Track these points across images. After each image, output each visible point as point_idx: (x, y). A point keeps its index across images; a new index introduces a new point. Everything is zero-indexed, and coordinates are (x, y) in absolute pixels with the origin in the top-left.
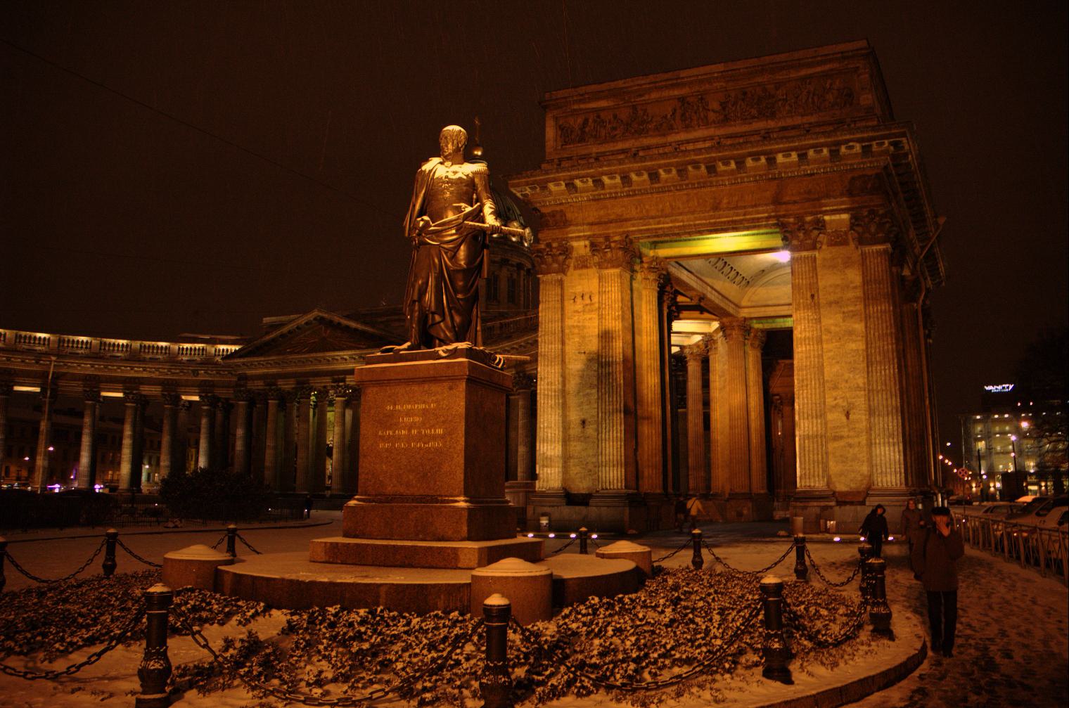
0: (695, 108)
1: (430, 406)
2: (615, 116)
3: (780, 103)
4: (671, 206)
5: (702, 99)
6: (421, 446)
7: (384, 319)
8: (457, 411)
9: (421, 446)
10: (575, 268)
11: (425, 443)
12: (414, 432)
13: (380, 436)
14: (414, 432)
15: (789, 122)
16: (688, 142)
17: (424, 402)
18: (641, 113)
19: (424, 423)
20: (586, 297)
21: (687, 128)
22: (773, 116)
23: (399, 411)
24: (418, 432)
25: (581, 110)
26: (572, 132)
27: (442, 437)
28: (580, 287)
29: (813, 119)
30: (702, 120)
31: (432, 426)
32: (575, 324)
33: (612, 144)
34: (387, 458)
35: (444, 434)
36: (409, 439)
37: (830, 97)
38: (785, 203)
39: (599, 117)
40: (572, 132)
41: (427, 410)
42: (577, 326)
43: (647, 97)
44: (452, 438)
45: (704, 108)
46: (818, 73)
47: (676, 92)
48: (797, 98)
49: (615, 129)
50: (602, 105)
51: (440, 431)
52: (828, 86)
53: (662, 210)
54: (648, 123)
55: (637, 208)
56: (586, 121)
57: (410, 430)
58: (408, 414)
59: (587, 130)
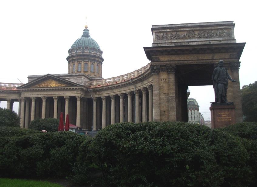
2: (171, 34)
7: (68, 77)
10: (161, 72)
12: (225, 118)
14: (225, 118)
15: (215, 39)
18: (178, 33)
19: (227, 116)
20: (165, 79)
21: (190, 38)
22: (211, 37)
25: (162, 31)
27: (231, 119)
29: (221, 39)
32: (162, 86)
36: (224, 119)
38: (215, 59)
39: (167, 33)
42: (162, 87)
43: (180, 30)
45: (194, 34)
46: (222, 28)
47: (187, 29)
49: (171, 37)
51: (230, 117)
52: (224, 31)
53: (184, 59)
56: (163, 34)
58: (223, 114)
59: (164, 36)
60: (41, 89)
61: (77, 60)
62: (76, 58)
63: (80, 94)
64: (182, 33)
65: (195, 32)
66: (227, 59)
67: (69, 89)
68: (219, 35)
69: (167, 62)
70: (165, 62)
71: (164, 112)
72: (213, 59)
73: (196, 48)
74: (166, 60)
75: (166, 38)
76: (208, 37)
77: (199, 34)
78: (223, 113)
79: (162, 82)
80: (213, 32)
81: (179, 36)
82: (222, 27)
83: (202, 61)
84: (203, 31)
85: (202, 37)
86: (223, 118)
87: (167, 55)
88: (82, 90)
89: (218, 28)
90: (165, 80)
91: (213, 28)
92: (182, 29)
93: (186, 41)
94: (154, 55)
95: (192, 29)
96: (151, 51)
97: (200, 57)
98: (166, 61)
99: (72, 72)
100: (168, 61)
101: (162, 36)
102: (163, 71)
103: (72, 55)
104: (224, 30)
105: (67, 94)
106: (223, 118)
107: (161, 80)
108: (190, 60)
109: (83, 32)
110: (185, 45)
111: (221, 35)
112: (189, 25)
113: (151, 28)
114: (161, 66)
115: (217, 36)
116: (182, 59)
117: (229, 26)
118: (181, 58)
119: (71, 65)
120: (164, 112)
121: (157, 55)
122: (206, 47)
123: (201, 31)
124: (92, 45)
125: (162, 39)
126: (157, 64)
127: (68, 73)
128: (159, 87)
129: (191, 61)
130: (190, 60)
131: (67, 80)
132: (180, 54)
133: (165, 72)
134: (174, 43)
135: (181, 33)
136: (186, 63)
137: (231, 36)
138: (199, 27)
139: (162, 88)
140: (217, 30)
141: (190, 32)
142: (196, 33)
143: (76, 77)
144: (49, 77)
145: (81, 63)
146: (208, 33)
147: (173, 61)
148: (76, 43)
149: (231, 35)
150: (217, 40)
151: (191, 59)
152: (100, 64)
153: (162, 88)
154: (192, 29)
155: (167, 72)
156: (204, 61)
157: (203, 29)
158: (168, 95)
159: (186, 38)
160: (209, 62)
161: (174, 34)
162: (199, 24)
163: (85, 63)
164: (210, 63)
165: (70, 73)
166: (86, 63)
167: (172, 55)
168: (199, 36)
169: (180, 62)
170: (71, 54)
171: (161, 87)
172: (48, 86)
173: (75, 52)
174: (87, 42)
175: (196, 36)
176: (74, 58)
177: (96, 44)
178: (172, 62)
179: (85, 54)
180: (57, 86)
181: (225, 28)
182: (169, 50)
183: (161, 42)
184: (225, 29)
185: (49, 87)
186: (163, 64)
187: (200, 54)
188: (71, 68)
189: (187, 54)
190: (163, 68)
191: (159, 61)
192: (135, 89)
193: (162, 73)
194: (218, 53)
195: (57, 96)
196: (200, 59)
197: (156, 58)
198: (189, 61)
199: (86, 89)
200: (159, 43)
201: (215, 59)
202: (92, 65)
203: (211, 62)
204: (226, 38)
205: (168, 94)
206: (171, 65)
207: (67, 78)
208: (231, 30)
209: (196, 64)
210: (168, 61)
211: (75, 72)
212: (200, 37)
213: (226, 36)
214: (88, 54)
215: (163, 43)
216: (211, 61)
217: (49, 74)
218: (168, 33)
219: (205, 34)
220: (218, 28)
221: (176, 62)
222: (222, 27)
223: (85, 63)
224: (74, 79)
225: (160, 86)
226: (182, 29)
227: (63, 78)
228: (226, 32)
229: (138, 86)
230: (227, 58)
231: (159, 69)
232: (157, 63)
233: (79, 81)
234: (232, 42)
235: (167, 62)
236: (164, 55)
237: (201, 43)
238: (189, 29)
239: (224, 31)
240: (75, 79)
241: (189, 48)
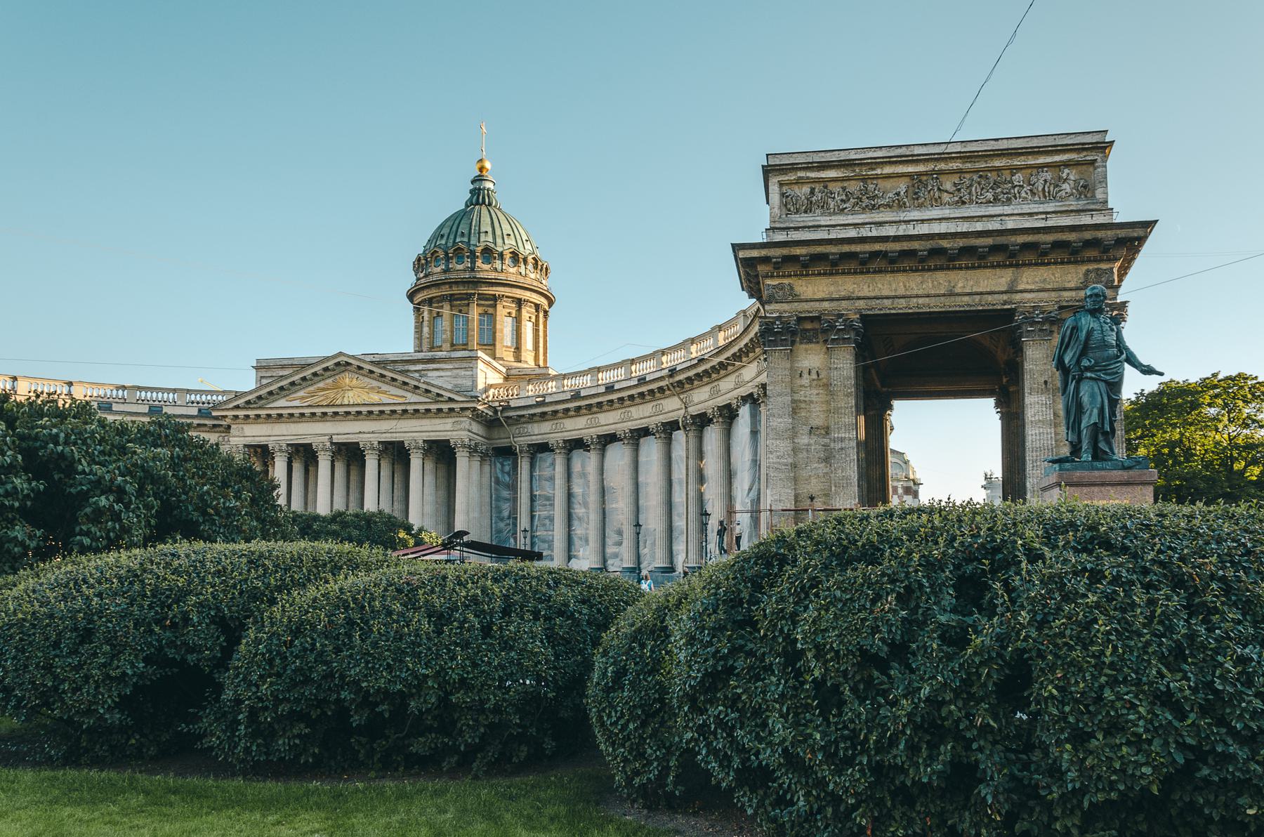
0: (930, 188)
2: (844, 189)
3: (1016, 189)
4: (905, 286)
5: (937, 178)
7: (419, 367)
10: (801, 343)
15: (1026, 209)
16: (923, 221)
18: (871, 187)
20: (814, 372)
21: (921, 206)
25: (808, 178)
26: (797, 200)
28: (806, 362)
29: (1050, 207)
30: (936, 200)
32: (802, 398)
33: (841, 217)
37: (1066, 187)
38: (1021, 292)
39: (826, 187)
40: (797, 200)
43: (879, 171)
45: (939, 189)
46: (1056, 162)
47: (910, 169)
48: (1033, 185)
50: (831, 176)
52: (1064, 175)
53: (896, 290)
54: (879, 198)
55: (869, 286)
59: (814, 199)
60: (313, 414)
61: (451, 298)
62: (445, 291)
63: (469, 431)
64: (888, 184)
65: (942, 178)
66: (1071, 289)
67: (423, 413)
68: (1044, 189)
69: (826, 305)
70: (817, 305)
71: (812, 498)
72: (1012, 290)
73: (945, 244)
74: (820, 295)
75: (823, 206)
76: (996, 199)
77: (959, 190)
79: (805, 380)
80: (1018, 178)
81: (873, 198)
82: (1057, 158)
83: (966, 299)
84: (975, 177)
85: (971, 201)
87: (825, 274)
88: (477, 416)
89: (1042, 160)
90: (815, 377)
91: (1017, 162)
92: (888, 170)
93: (903, 216)
94: (772, 276)
95: (930, 166)
96: (766, 260)
97: (960, 285)
98: (822, 300)
99: (432, 349)
100: (832, 300)
101: (808, 199)
102: (810, 342)
103: (431, 279)
104: (1066, 171)
105: (414, 432)
107: (801, 376)
108: (917, 296)
109: (472, 187)
110: (901, 233)
111: (1049, 192)
112: (918, 151)
113: (763, 166)
114: (800, 319)
115: (1033, 194)
116: (886, 293)
117: (1085, 153)
118: (880, 286)
119: (426, 318)
120: (812, 498)
121: (784, 276)
122: (989, 241)
123: (968, 176)
124: (506, 242)
125: (806, 212)
126: (785, 312)
127: (415, 352)
128: (793, 401)
129: (921, 301)
130: (917, 296)
131: (412, 378)
132: (880, 271)
133: (818, 342)
134: (855, 225)
135: (881, 183)
136: (901, 306)
137: (1094, 196)
138: (960, 158)
139: (803, 405)
140: (1035, 171)
141: (924, 178)
142: (948, 186)
143: (450, 366)
144: (341, 365)
145: (464, 308)
146: (997, 184)
147: (848, 299)
148: (445, 231)
149: (1095, 189)
150: (1031, 214)
151: (920, 292)
152: (541, 315)
153: (803, 405)
154: (930, 166)
155: (825, 341)
156: (977, 298)
157: (977, 165)
158: (827, 433)
159: (901, 206)
160: (996, 302)
161: (854, 187)
162: (958, 148)
163: (481, 310)
164: (999, 308)
165: (424, 349)
166: (486, 313)
167: (843, 273)
168: (956, 199)
169: (878, 301)
170: (426, 276)
171: (800, 401)
172: (338, 402)
173: (439, 269)
174: (490, 230)
175: (946, 198)
176: (434, 293)
177: (525, 238)
178: (844, 304)
179: (481, 275)
180: (375, 398)
181: (1070, 160)
182: (833, 254)
183: (802, 224)
184: (1067, 164)
185: (342, 405)
186: (809, 312)
187: (960, 268)
188: (426, 330)
189: (905, 271)
190: (808, 326)
191: (796, 298)
192: (683, 411)
193: (803, 346)
194: (1036, 264)
195: (375, 439)
196: (958, 290)
197: (781, 287)
198: (915, 300)
199: (490, 413)
200: (796, 229)
201: (1021, 292)
203: (1005, 303)
204: (1073, 204)
205: (827, 430)
206: (840, 316)
207: (412, 368)
208: (1095, 169)
209: (944, 310)
210: (832, 300)
211: (441, 346)
212: (964, 203)
213: (1072, 194)
215: (809, 227)
216: (1005, 297)
217: (341, 354)
218: (831, 186)
219: (982, 189)
220: (1042, 160)
221: (861, 304)
222: (1057, 158)
224: (442, 373)
225: (796, 397)
226: (888, 170)
227: (400, 367)
228: (1072, 177)
229: (696, 400)
230: (1072, 285)
231: (794, 333)
232: (785, 307)
233: (460, 381)
234: (1099, 219)
235: (826, 305)
236: (812, 275)
237: (964, 227)
238: (921, 168)
239: (1064, 175)
240: (449, 373)
241: (916, 245)
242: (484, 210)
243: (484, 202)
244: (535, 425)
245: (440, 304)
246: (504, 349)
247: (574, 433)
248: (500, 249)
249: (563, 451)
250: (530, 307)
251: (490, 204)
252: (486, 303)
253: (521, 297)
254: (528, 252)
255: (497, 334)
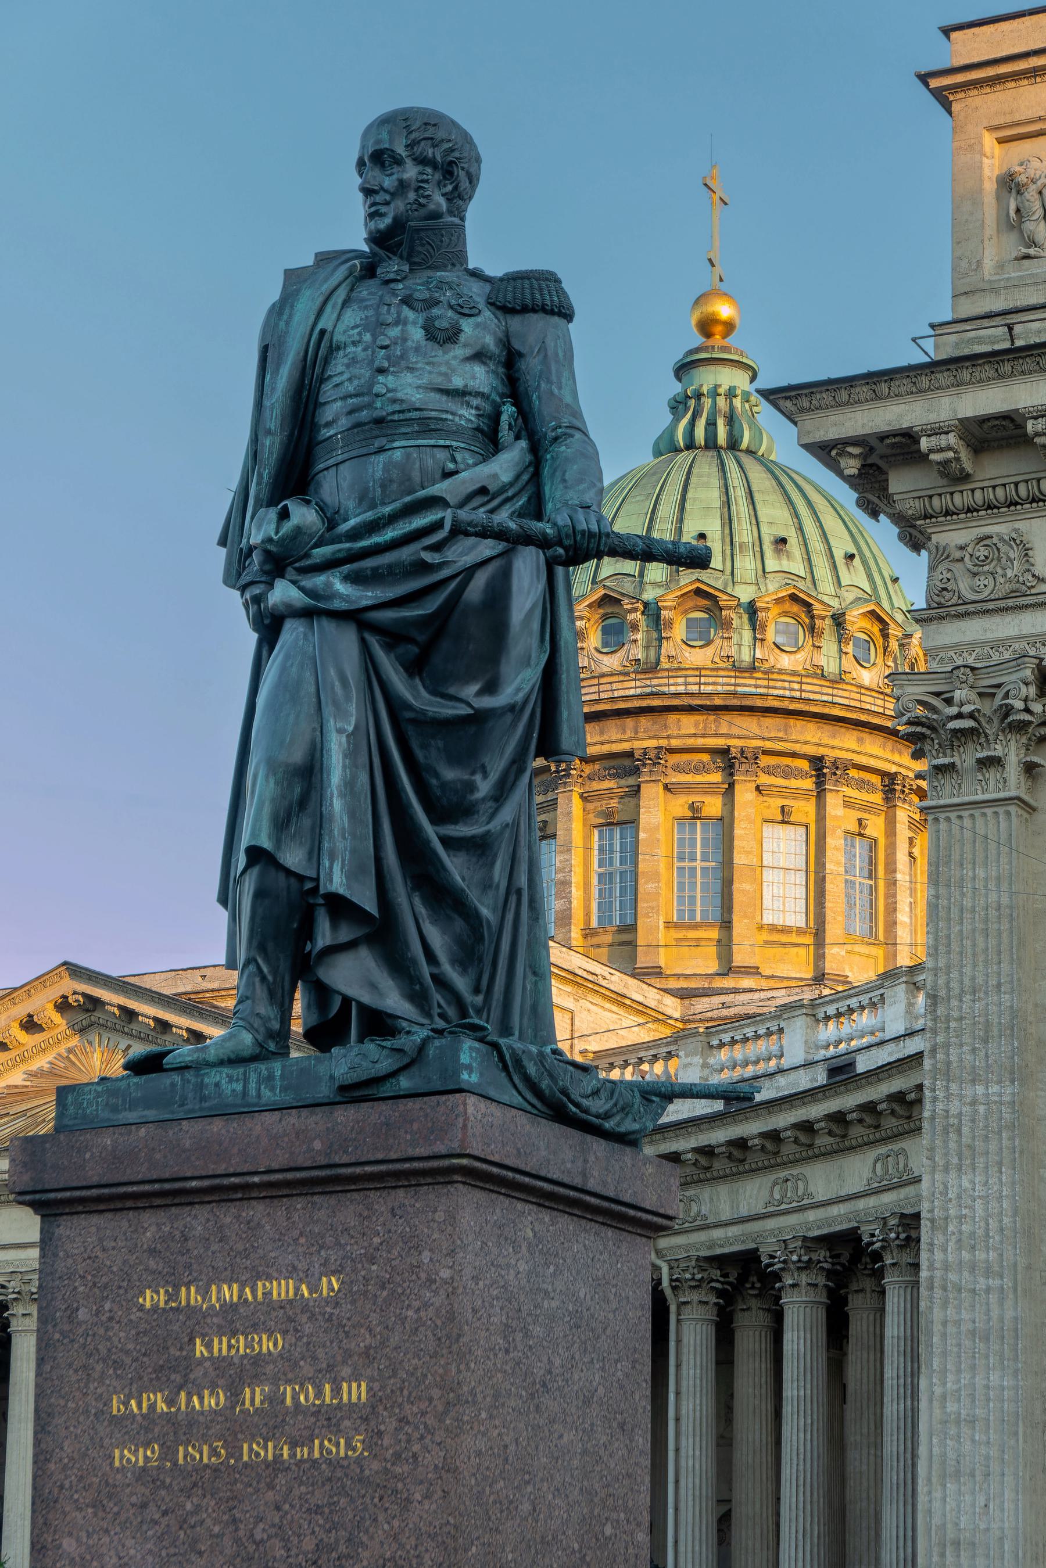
1: (314, 1288)
6: (278, 1457)
8: (426, 1305)
9: (278, 1457)
11: (293, 1445)
12: (254, 1397)
13: (116, 1421)
14: (254, 1397)
17: (292, 1271)
23: (191, 1311)
24: (268, 1399)
31: (331, 1373)
34: (144, 1506)
35: (375, 1399)
41: (305, 1307)
44: (403, 1420)
51: (356, 1392)
57: (235, 1395)
78: (229, 1293)
86: (211, 1401)
106: (211, 1401)
124: (771, 564)
163: (680, 805)
202: (781, 830)
214: (717, 686)
223: (680, 805)
242: (706, 467)
243: (711, 444)
244: (723, 1190)
245: (550, 796)
246: (765, 936)
247: (835, 1210)
248: (745, 594)
249: (804, 1279)
250: (861, 785)
251: (733, 445)
252: (699, 779)
253: (822, 751)
254: (850, 596)
255: (736, 886)
